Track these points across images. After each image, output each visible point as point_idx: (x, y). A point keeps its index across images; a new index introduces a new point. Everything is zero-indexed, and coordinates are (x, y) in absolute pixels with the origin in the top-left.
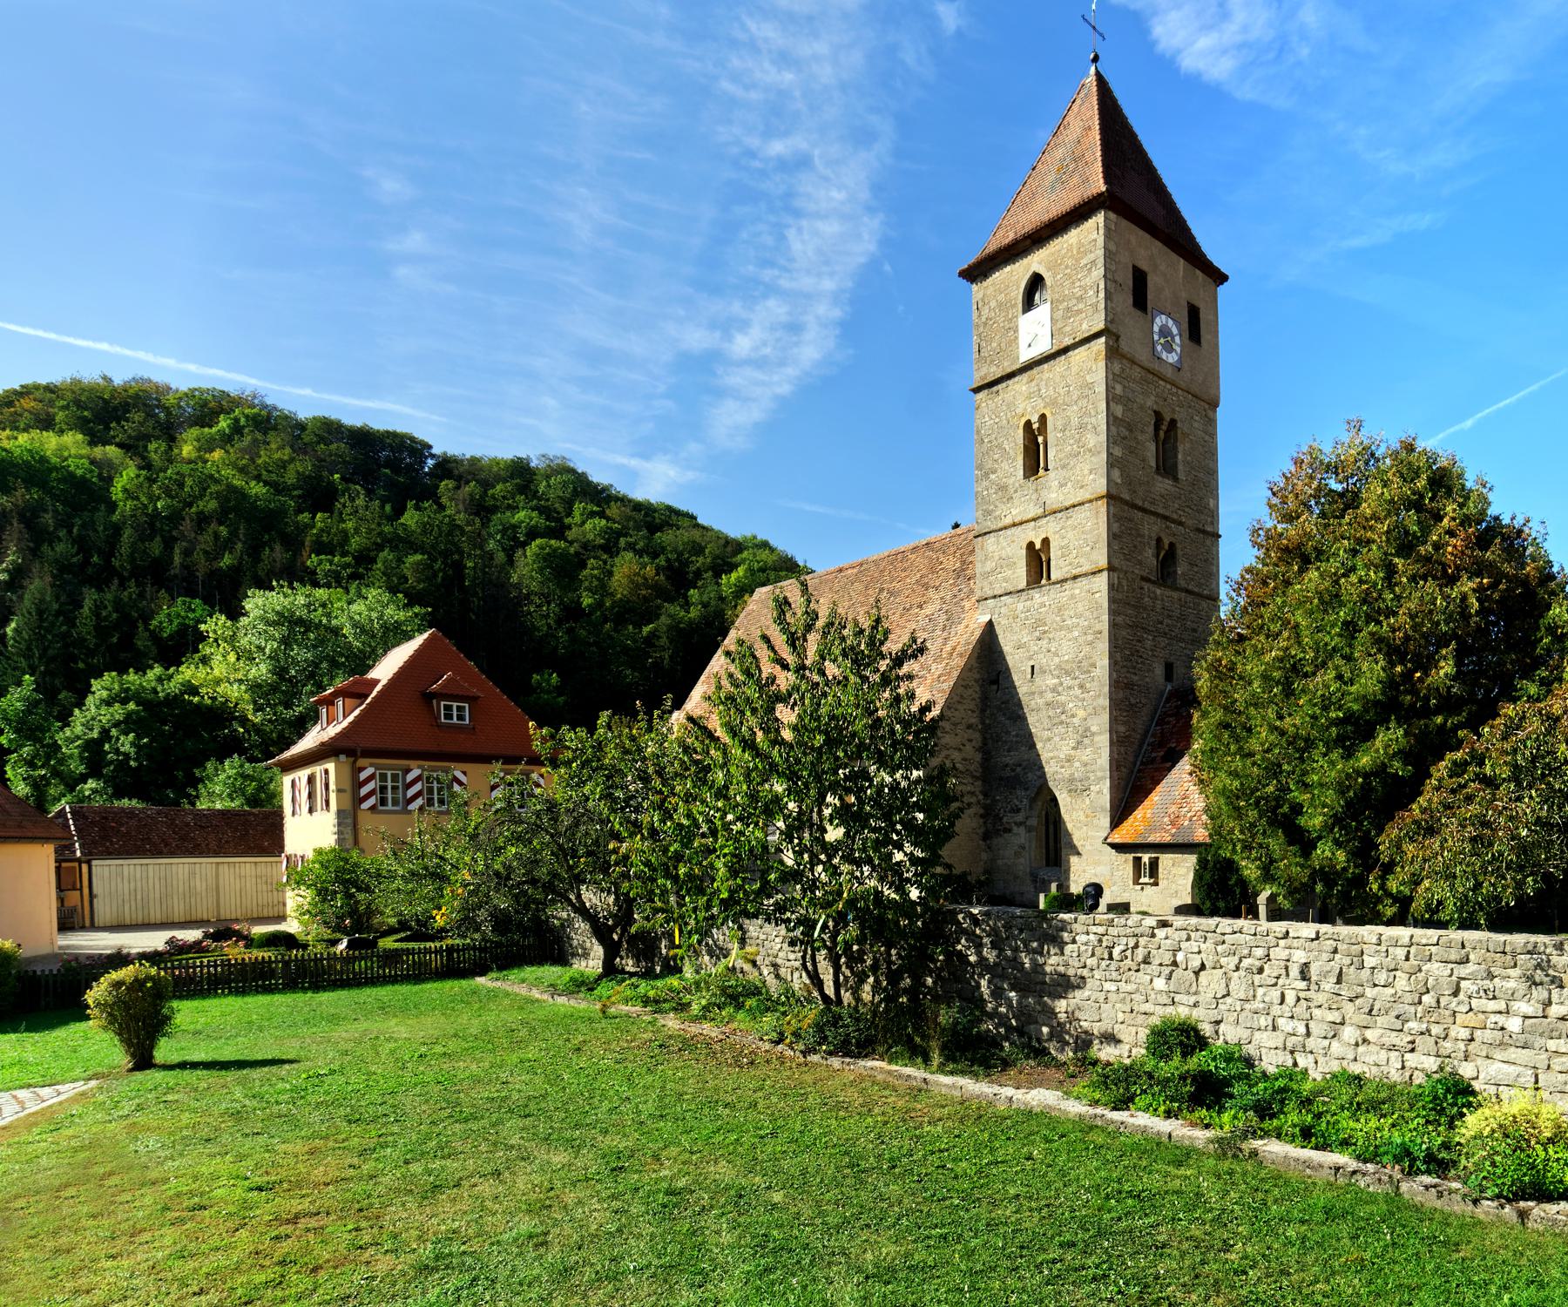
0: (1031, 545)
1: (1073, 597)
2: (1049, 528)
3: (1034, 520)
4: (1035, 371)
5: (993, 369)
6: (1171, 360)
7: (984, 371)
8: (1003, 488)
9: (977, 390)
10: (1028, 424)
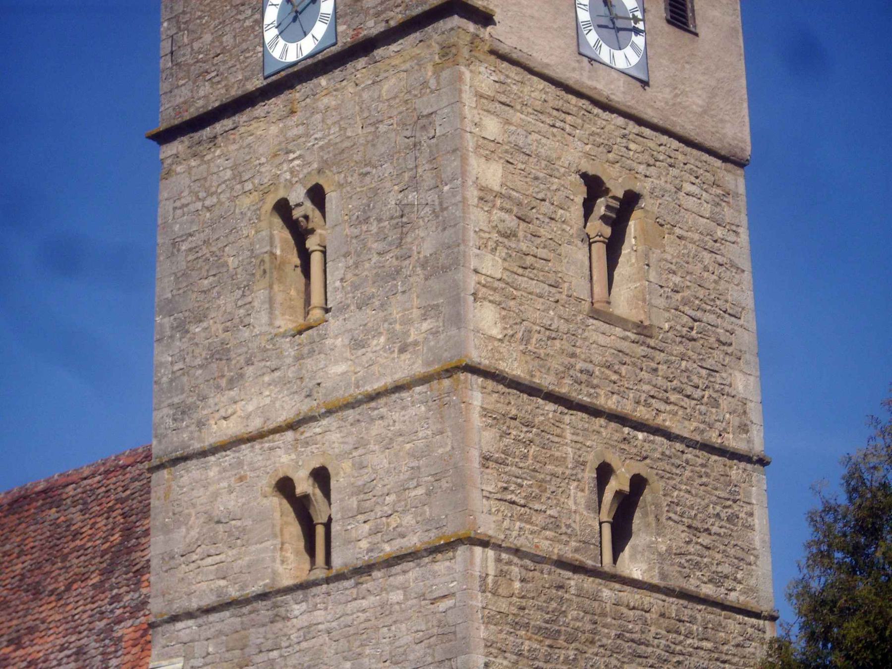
0: (285, 486)
1: (385, 609)
2: (330, 441)
3: (292, 426)
4: (302, 90)
5: (205, 89)
6: (621, 64)
7: (183, 94)
8: (220, 353)
9: (165, 136)
10: (283, 208)
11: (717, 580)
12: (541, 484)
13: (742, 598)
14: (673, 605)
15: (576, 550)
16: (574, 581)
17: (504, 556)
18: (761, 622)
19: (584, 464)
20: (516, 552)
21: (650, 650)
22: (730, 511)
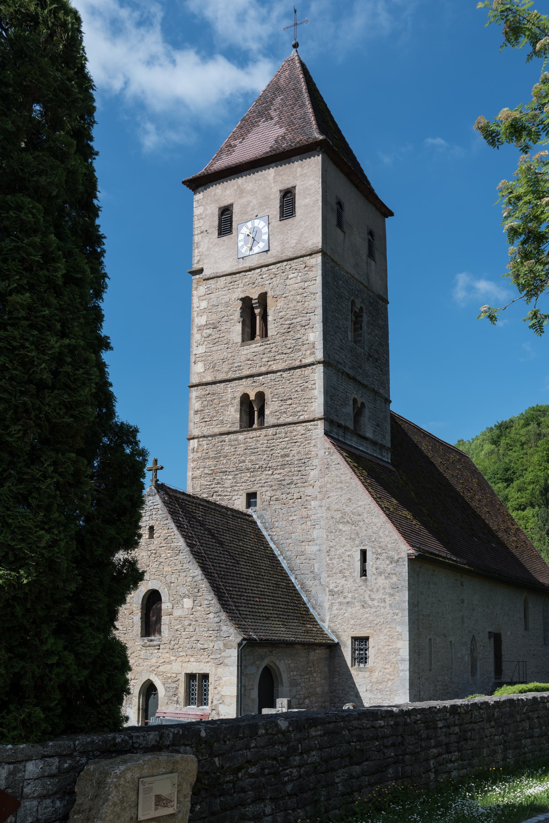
11: (294, 414)
12: (217, 412)
13: (306, 417)
14: (271, 431)
15: (230, 427)
16: (227, 438)
17: (201, 439)
18: (316, 422)
19: (235, 398)
20: (204, 437)
21: (259, 449)
22: (302, 387)
